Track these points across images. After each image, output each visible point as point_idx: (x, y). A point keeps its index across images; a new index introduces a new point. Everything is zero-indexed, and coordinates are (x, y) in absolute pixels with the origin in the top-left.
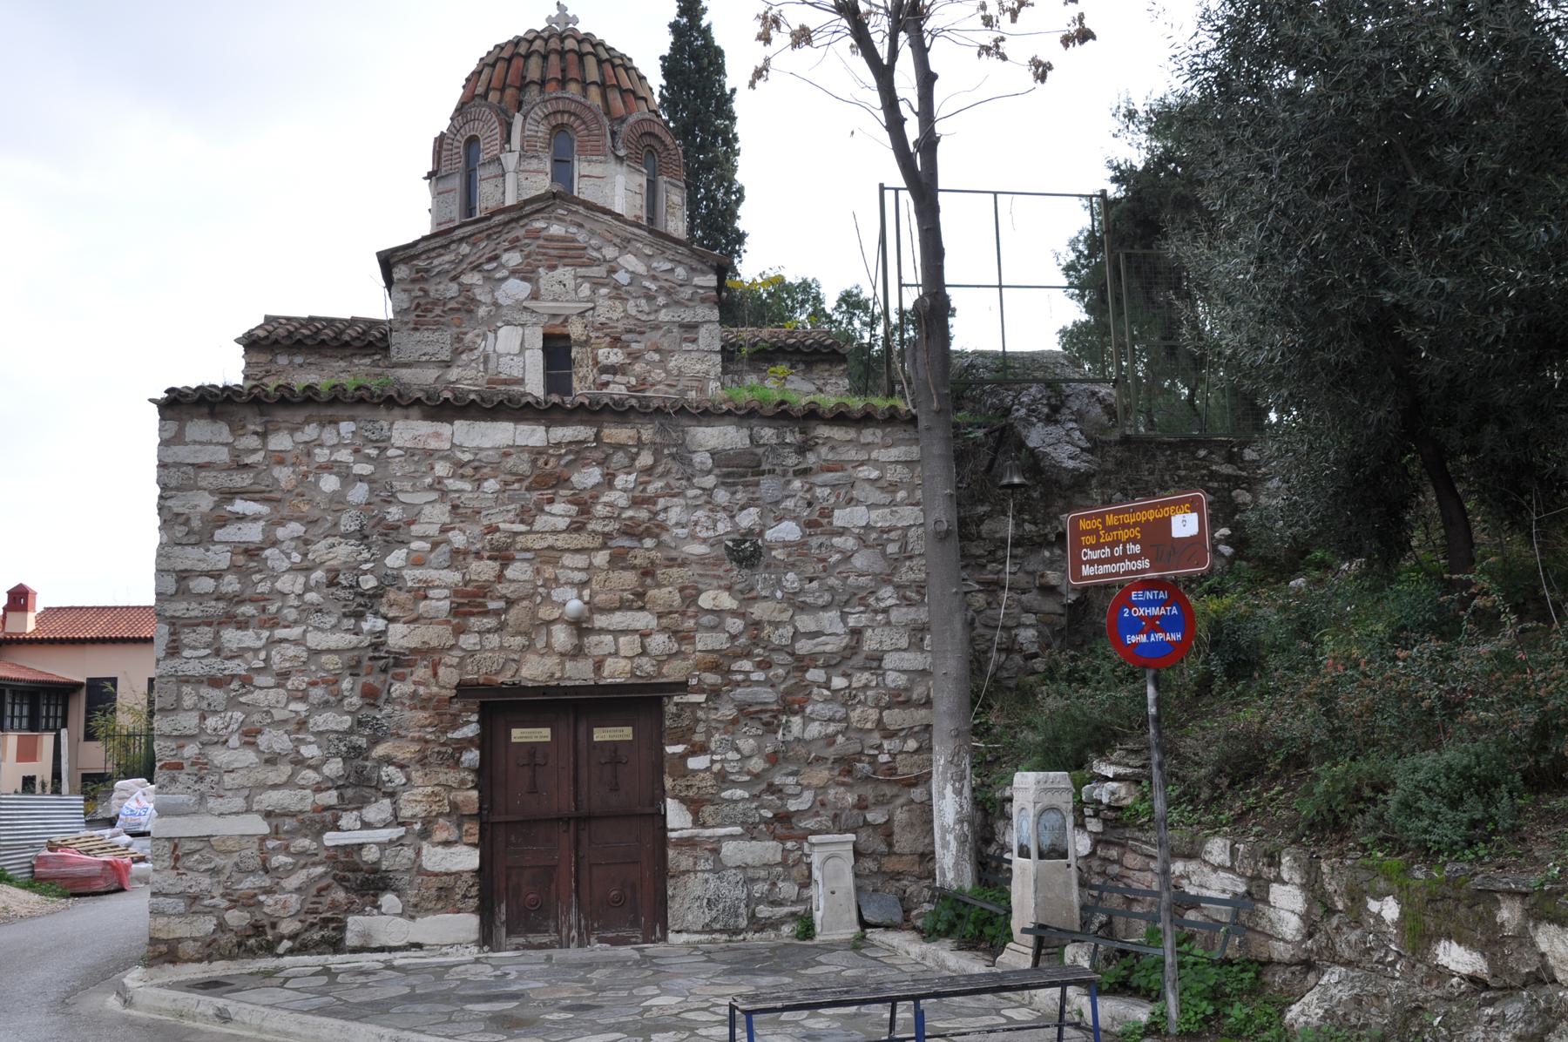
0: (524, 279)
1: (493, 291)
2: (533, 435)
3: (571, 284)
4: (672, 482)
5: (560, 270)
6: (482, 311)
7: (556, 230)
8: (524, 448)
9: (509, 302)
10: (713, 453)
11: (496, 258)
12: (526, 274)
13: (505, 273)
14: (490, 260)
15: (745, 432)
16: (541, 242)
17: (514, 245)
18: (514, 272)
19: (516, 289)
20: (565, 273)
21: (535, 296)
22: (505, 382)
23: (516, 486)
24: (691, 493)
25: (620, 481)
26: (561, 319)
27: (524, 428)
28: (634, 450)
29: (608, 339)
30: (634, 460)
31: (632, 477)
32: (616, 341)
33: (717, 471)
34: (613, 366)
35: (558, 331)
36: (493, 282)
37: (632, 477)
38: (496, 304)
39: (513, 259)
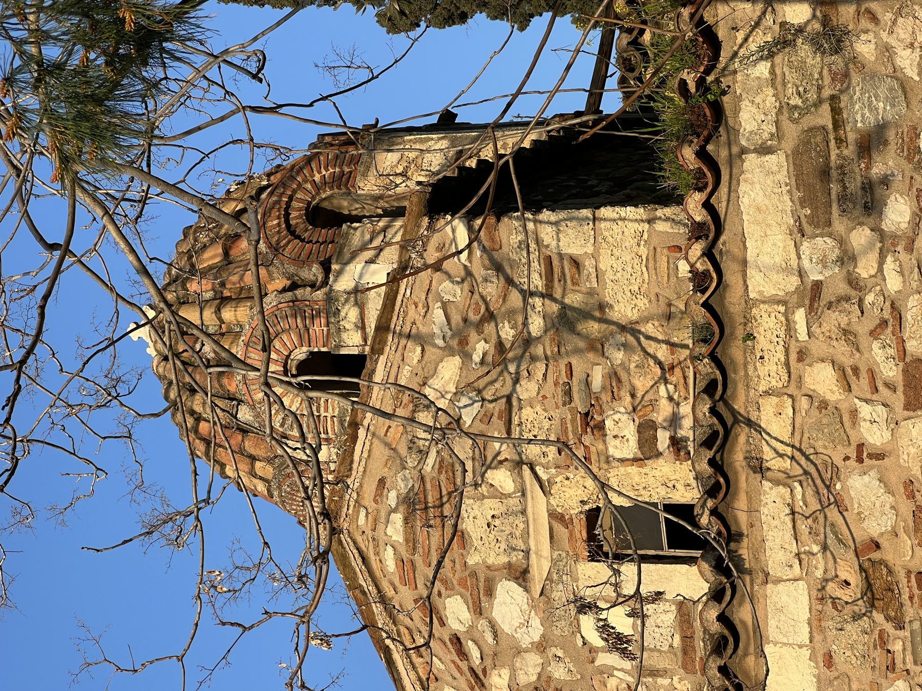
0: (490, 592)
1: (519, 651)
2: (785, 610)
3: (491, 506)
4: (869, 323)
5: (467, 525)
6: (559, 672)
7: (395, 530)
8: (816, 623)
9: (536, 622)
10: (800, 232)
11: (456, 640)
12: (480, 594)
13: (482, 624)
14: (462, 653)
15: (751, 160)
16: (418, 559)
17: (431, 610)
18: (478, 610)
19: (510, 605)
20: (476, 515)
21: (521, 576)
22: (687, 639)
23: (897, 647)
24: (894, 283)
25: (875, 436)
26: (558, 527)
27: (773, 628)
28: (804, 403)
29: (587, 439)
30: (824, 405)
31: (865, 410)
32: (591, 423)
33: (839, 225)
34: (641, 429)
35: (581, 532)
36: (504, 650)
37: (865, 410)
38: (541, 647)
39: (456, 611)
